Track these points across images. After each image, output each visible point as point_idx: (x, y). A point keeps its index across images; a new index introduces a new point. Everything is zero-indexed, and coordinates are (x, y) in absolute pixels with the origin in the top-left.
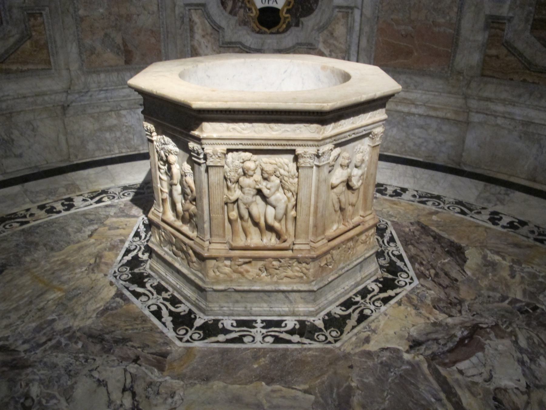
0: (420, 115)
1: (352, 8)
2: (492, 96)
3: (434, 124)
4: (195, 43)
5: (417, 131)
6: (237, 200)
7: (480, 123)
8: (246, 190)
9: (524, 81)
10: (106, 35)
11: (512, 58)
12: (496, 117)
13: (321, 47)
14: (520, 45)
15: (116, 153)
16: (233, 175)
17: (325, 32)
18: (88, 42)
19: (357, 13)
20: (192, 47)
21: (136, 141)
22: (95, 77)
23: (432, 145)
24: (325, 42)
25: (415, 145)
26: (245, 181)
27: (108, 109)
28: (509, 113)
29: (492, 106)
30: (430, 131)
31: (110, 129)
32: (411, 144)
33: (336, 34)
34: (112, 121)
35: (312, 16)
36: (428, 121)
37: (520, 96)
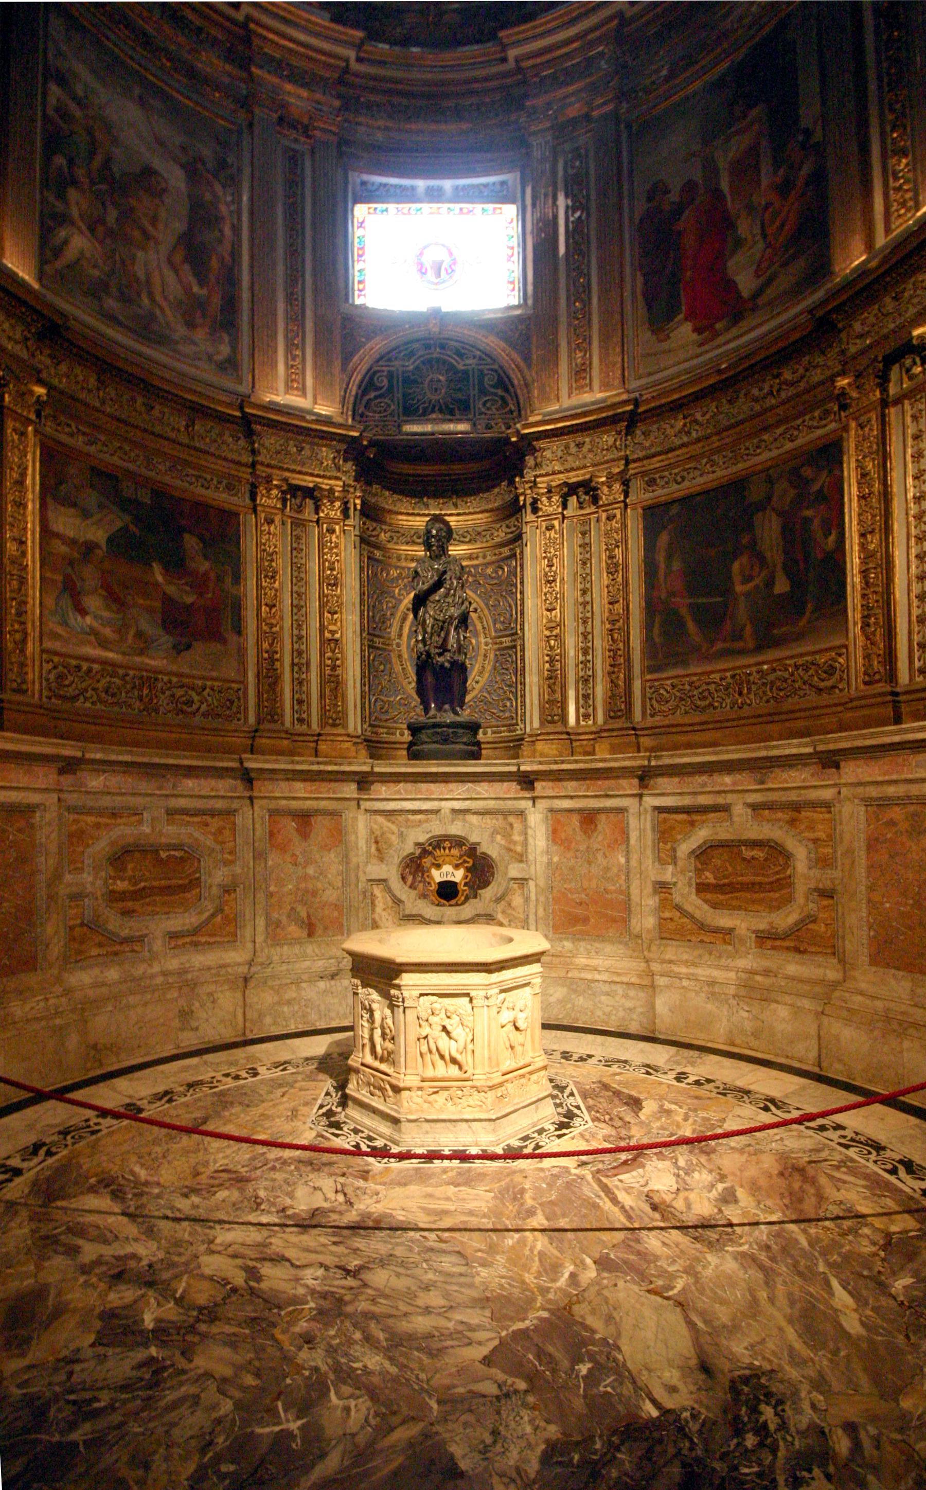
0: (605, 982)
1: (526, 880)
2: (673, 958)
3: (620, 990)
4: (376, 917)
5: (603, 998)
6: (426, 1037)
7: (667, 987)
8: (434, 1026)
9: (702, 941)
10: (292, 909)
11: (686, 920)
12: (680, 979)
13: (500, 917)
14: (690, 909)
15: (292, 1028)
16: (424, 1015)
17: (503, 903)
18: (275, 915)
19: (531, 883)
20: (373, 919)
21: (313, 1016)
22: (278, 948)
23: (621, 1014)
24: (503, 912)
25: (604, 1014)
26: (433, 1019)
27: (288, 981)
28: (693, 974)
29: (676, 969)
30: (617, 998)
31: (289, 1003)
32: (599, 1013)
33: (514, 904)
34: (291, 994)
35: (489, 888)
36: (614, 987)
37: (700, 956)
